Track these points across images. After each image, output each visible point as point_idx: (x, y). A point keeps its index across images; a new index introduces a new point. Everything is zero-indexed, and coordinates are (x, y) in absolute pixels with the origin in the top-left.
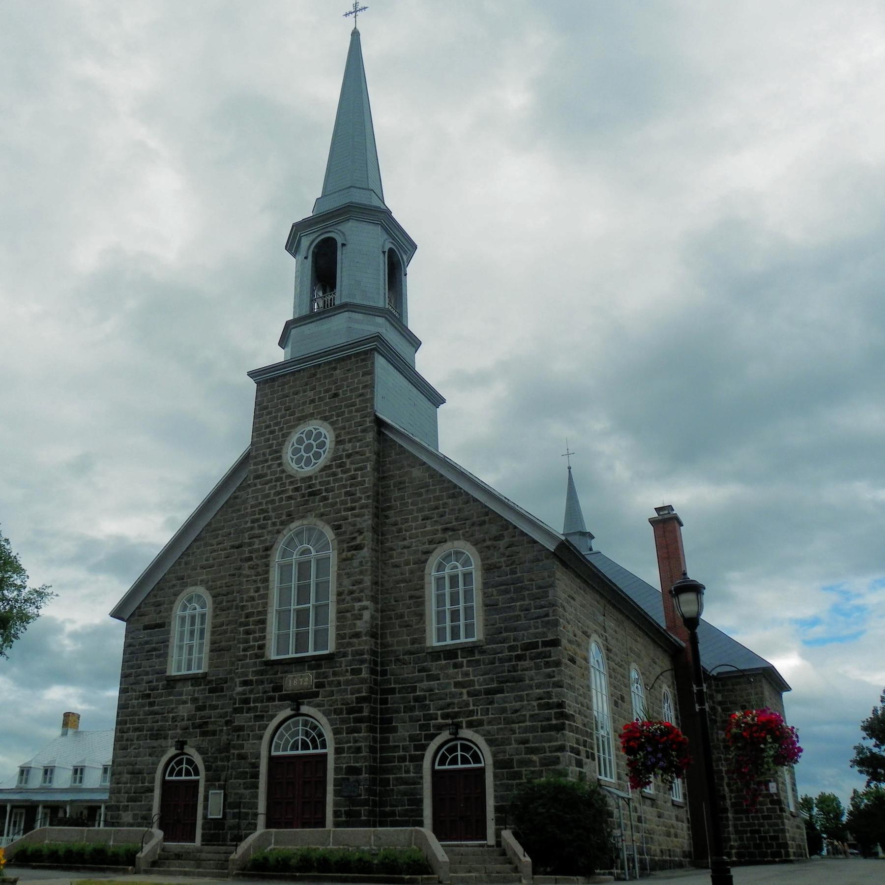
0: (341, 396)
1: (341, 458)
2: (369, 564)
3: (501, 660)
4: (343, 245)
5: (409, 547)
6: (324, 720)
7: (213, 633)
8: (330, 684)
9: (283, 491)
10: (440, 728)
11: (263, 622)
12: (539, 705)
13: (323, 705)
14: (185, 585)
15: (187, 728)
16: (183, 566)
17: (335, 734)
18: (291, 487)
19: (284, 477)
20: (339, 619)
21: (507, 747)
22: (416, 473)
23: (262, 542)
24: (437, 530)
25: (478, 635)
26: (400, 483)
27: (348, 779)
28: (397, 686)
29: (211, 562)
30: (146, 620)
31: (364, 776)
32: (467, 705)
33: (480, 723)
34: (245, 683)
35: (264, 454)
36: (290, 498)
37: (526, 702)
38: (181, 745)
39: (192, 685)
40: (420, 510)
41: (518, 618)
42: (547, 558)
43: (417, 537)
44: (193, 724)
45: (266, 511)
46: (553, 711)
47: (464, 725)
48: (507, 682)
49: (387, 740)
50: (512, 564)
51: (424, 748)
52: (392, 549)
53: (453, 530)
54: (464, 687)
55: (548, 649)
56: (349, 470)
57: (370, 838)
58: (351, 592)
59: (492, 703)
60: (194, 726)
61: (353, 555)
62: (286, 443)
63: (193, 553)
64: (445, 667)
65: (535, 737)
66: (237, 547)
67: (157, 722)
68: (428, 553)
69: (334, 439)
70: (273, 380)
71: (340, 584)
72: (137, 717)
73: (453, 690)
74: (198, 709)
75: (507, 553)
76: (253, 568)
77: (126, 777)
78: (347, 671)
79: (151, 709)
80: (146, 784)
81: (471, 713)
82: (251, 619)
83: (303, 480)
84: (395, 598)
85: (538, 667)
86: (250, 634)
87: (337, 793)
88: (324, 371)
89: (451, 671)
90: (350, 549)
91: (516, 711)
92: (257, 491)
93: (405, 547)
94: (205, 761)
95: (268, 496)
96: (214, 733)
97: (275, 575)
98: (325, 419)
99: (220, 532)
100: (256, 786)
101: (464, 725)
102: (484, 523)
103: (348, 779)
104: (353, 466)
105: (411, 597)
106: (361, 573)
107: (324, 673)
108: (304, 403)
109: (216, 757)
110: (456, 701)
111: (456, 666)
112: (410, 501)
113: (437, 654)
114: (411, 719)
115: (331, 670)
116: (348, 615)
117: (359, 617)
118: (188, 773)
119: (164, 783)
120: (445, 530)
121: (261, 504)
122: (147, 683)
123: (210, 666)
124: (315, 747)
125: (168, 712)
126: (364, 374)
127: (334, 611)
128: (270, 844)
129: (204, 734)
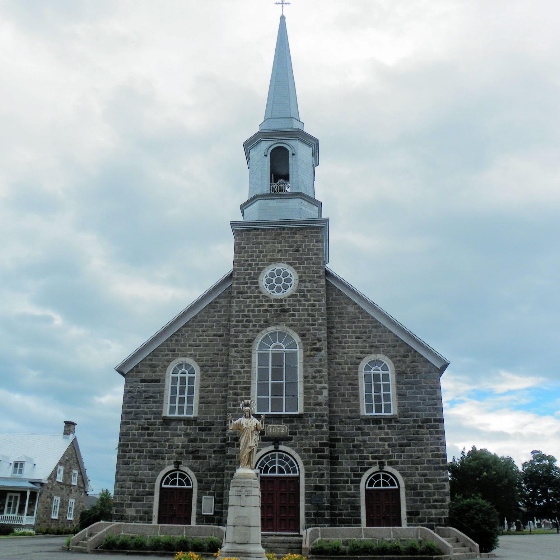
0: (301, 252)
1: (303, 291)
2: (326, 361)
3: (409, 428)
4: (293, 154)
5: (347, 354)
6: (297, 456)
7: (201, 391)
8: (301, 433)
9: (261, 305)
10: (371, 465)
11: (248, 389)
12: (432, 455)
13: (296, 446)
14: (176, 356)
15: (181, 453)
16: (174, 342)
17: (305, 465)
18: (266, 304)
19: (259, 295)
20: (305, 393)
21: (414, 478)
22: (350, 309)
23: (244, 336)
24: (366, 346)
25: (394, 411)
26: (340, 313)
27: (315, 493)
28: (341, 437)
29: (198, 343)
30: (143, 376)
31: (327, 491)
32: (388, 452)
33: (397, 463)
35: (244, 279)
36: (267, 311)
38: (177, 464)
39: (185, 425)
40: (354, 332)
41: (418, 404)
42: (435, 372)
43: (353, 348)
44: (186, 451)
45: (248, 316)
47: (386, 464)
48: (413, 440)
49: (336, 470)
50: (414, 373)
51: (361, 476)
52: (335, 353)
53: (376, 347)
54: (386, 441)
55: (437, 423)
56: (309, 300)
57: (390, 533)
58: (314, 377)
59: (403, 452)
60: (187, 452)
61: (315, 354)
62: (262, 274)
63: (182, 335)
65: (430, 473)
66: (219, 336)
67: (155, 447)
68: (361, 359)
69: (297, 278)
70: (249, 230)
71: (305, 371)
72: (137, 443)
73: (379, 442)
74: (191, 441)
75: (411, 365)
76: (238, 352)
77: (129, 483)
78: (312, 426)
79: (150, 438)
80: (147, 490)
81: (391, 457)
82: (239, 386)
83: (276, 300)
84: (338, 383)
85: (431, 433)
86: (238, 395)
87: (307, 501)
88: (287, 234)
89: (377, 431)
90: (312, 350)
91: (419, 457)
92: (241, 301)
93: (345, 353)
94: (197, 476)
95: (249, 306)
96: (205, 458)
97: (255, 359)
98: (291, 264)
99: (205, 324)
101: (386, 464)
103: (315, 493)
104: (312, 298)
105: (350, 384)
106: (321, 366)
107: (296, 426)
108: (274, 251)
109: (207, 474)
110: (381, 449)
111: (380, 428)
112: (347, 325)
113: (367, 421)
114: (352, 458)
115: (301, 425)
116: (312, 391)
117: (321, 393)
119: (161, 489)
120: (372, 347)
121: (244, 311)
122: (146, 419)
123: (199, 413)
124: (289, 472)
125: (165, 441)
126: (317, 241)
127: (302, 388)
128: (318, 537)
129: (194, 458)
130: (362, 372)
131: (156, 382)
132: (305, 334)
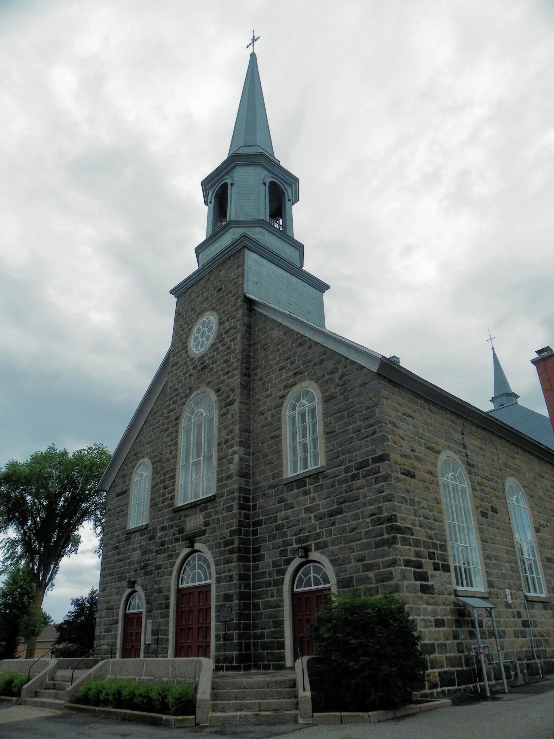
3: (340, 483)
25: (322, 462)
32: (315, 528)
34: (163, 529)
37: (361, 520)
41: (351, 440)
46: (384, 526)
47: (313, 548)
48: (345, 502)
49: (256, 568)
51: (282, 572)
54: (312, 512)
59: (333, 524)
64: (298, 495)
68: (283, 397)
73: (304, 515)
75: (341, 383)
81: (318, 535)
87: (218, 618)
89: (302, 498)
91: (353, 529)
100: (167, 616)
101: (313, 548)
102: (323, 360)
103: (225, 604)
105: (272, 438)
111: (305, 493)
131: (125, 494)
132: (219, 388)
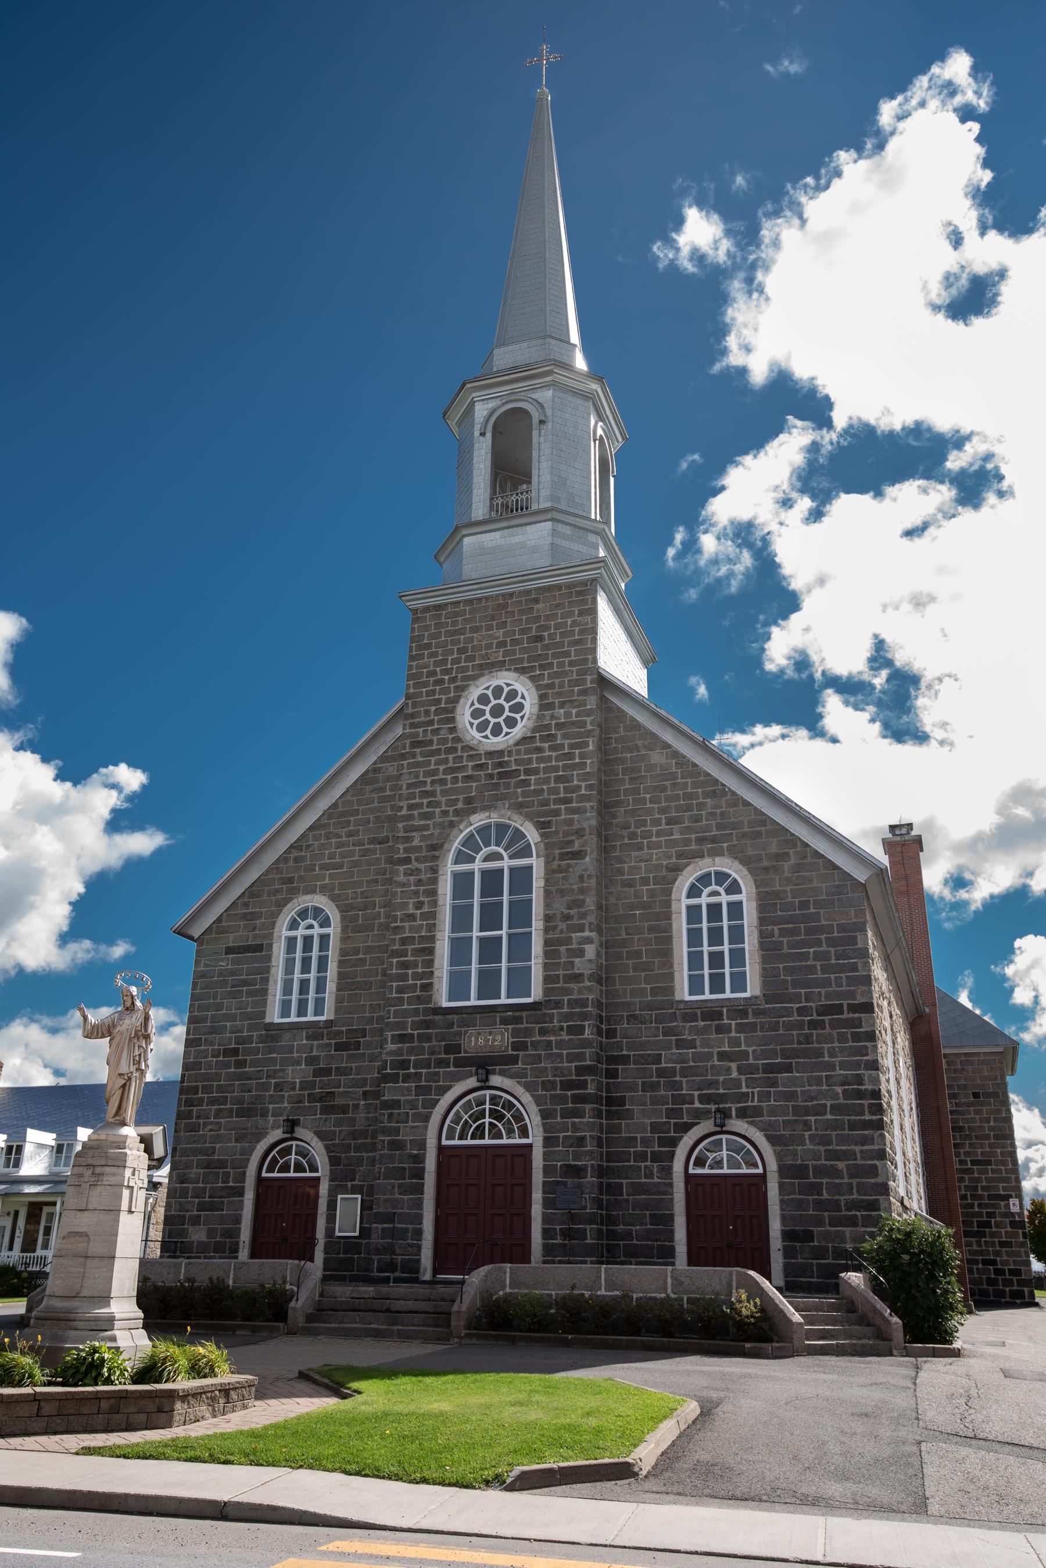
1: (547, 727)
3: (789, 1026)
6: (526, 1098)
7: (341, 964)
8: (535, 1045)
9: (458, 768)
10: (699, 1115)
11: (431, 951)
12: (844, 1092)
14: (294, 892)
16: (291, 863)
17: (543, 1118)
18: (470, 764)
19: (456, 744)
20: (547, 954)
22: (657, 757)
23: (423, 838)
25: (753, 988)
27: (565, 1184)
30: (231, 940)
33: (757, 1112)
34: (402, 1038)
36: (468, 778)
37: (825, 1087)
40: (663, 810)
41: (812, 969)
43: (660, 847)
45: (432, 793)
46: (866, 1102)
47: (734, 1113)
51: (674, 1143)
54: (732, 1061)
55: (857, 1015)
58: (567, 918)
59: (774, 1084)
61: (569, 866)
62: (462, 700)
64: (705, 1030)
69: (536, 701)
71: (547, 905)
74: (318, 1073)
77: (194, 1172)
78: (561, 1028)
82: (410, 947)
83: (490, 754)
85: (842, 1038)
87: (547, 1203)
90: (563, 856)
92: (418, 765)
95: (435, 772)
96: (344, 1109)
97: (446, 888)
98: (522, 671)
99: (352, 819)
100: (420, 1189)
101: (734, 1113)
102: (759, 834)
103: (565, 1184)
105: (651, 930)
107: (527, 1029)
111: (720, 1029)
118: (299, 1168)
119: (260, 1180)
120: (701, 840)
123: (338, 1010)
125: (268, 1077)
127: (541, 942)
129: (327, 1110)
130: (682, 902)
131: (255, 952)
132: (549, 822)
